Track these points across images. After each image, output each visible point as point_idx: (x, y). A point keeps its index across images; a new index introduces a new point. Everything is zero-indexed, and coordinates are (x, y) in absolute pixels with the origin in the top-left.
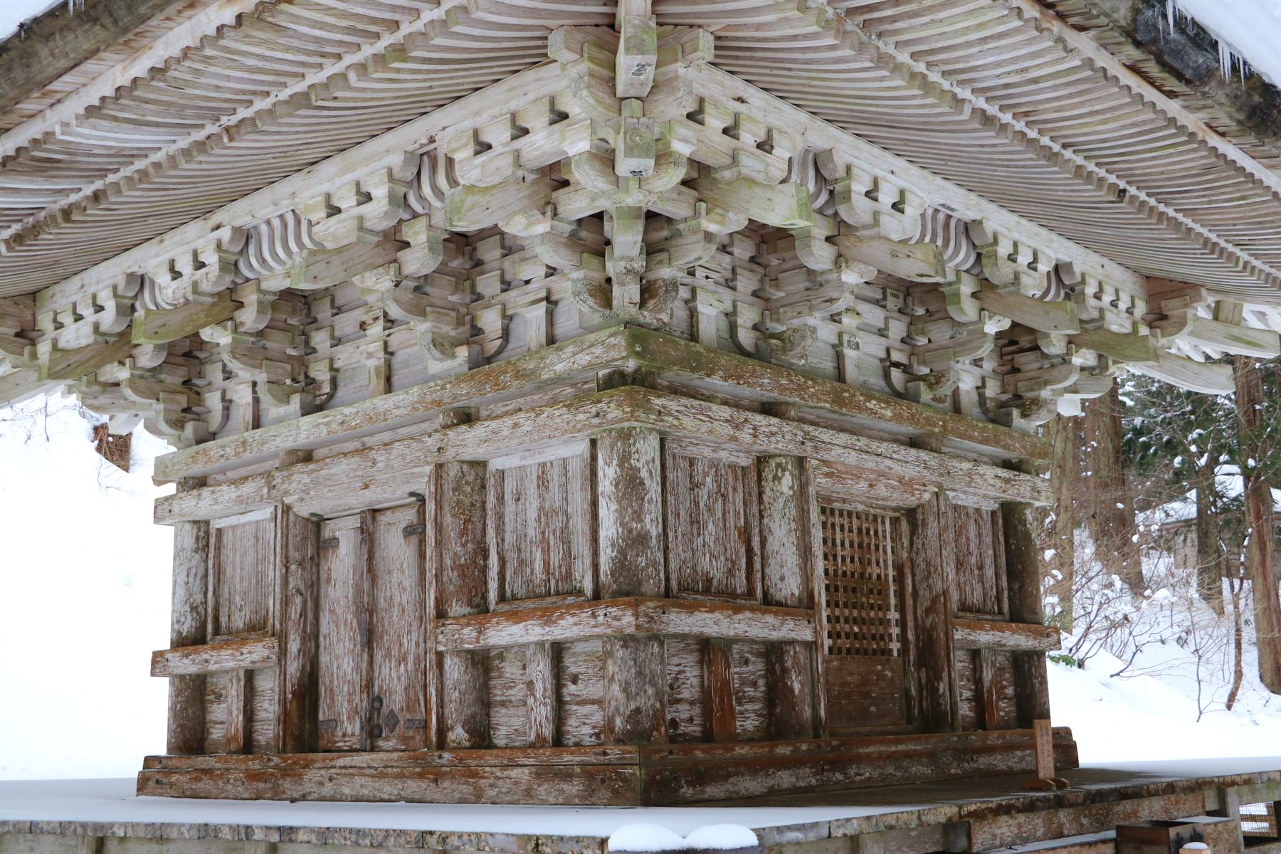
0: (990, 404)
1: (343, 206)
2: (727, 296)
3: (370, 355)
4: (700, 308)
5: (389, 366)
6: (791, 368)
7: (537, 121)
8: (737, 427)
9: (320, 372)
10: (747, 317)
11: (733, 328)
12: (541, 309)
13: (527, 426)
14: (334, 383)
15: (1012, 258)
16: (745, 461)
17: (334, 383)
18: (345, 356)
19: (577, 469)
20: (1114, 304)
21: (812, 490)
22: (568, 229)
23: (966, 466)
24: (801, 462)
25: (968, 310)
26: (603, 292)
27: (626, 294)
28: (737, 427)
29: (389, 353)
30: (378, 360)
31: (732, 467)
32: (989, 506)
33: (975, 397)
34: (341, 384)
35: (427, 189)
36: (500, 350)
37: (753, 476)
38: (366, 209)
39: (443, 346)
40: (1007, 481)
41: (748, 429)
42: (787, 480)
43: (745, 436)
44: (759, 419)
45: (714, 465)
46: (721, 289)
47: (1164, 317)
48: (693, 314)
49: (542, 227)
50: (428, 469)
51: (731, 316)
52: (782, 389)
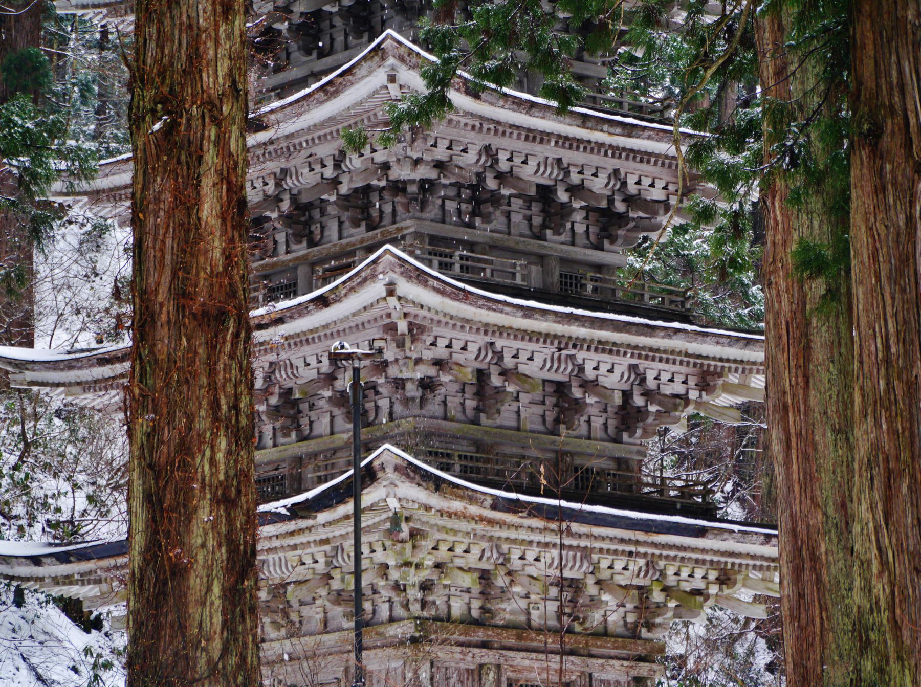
0: (629, 625)
1: (307, 562)
2: (466, 596)
3: (317, 613)
4: (452, 604)
5: (326, 617)
6: (497, 626)
7: (379, 550)
8: (464, 655)
9: (294, 617)
10: (476, 604)
11: (469, 609)
12: (387, 605)
13: (380, 655)
14: (301, 622)
15: (611, 567)
16: (472, 667)
17: (301, 622)
18: (306, 611)
19: (400, 670)
20: (691, 576)
21: (504, 679)
22: (392, 583)
23: (600, 661)
24: (498, 667)
25: (592, 590)
26: (406, 606)
27: (415, 608)
28: (464, 655)
29: (326, 613)
30: (321, 616)
31: (467, 670)
32: (623, 679)
33: (622, 622)
34: (305, 623)
35: (340, 559)
36: (372, 618)
37: (476, 672)
38: (315, 565)
39: (346, 616)
40: (632, 667)
41: (470, 655)
42: (492, 674)
43: (469, 658)
44: (476, 650)
45: (458, 669)
46: (463, 594)
47: (729, 579)
48: (449, 607)
49: (382, 583)
50: (342, 669)
51: (469, 604)
52: (489, 636)
